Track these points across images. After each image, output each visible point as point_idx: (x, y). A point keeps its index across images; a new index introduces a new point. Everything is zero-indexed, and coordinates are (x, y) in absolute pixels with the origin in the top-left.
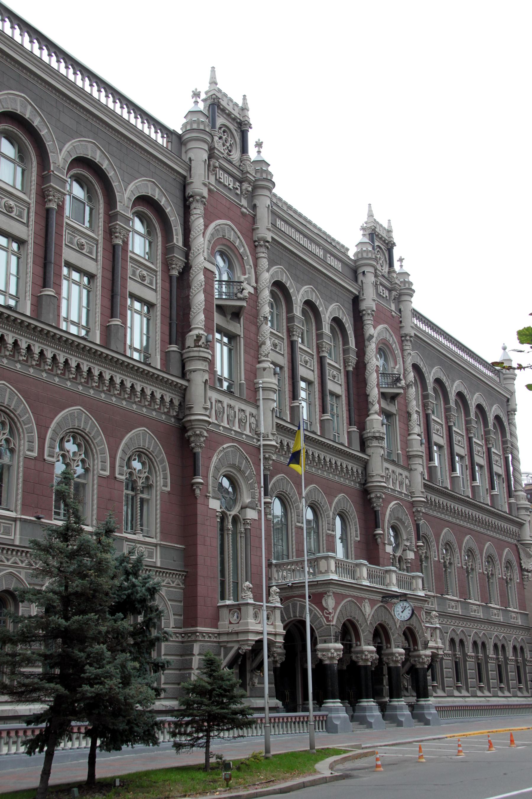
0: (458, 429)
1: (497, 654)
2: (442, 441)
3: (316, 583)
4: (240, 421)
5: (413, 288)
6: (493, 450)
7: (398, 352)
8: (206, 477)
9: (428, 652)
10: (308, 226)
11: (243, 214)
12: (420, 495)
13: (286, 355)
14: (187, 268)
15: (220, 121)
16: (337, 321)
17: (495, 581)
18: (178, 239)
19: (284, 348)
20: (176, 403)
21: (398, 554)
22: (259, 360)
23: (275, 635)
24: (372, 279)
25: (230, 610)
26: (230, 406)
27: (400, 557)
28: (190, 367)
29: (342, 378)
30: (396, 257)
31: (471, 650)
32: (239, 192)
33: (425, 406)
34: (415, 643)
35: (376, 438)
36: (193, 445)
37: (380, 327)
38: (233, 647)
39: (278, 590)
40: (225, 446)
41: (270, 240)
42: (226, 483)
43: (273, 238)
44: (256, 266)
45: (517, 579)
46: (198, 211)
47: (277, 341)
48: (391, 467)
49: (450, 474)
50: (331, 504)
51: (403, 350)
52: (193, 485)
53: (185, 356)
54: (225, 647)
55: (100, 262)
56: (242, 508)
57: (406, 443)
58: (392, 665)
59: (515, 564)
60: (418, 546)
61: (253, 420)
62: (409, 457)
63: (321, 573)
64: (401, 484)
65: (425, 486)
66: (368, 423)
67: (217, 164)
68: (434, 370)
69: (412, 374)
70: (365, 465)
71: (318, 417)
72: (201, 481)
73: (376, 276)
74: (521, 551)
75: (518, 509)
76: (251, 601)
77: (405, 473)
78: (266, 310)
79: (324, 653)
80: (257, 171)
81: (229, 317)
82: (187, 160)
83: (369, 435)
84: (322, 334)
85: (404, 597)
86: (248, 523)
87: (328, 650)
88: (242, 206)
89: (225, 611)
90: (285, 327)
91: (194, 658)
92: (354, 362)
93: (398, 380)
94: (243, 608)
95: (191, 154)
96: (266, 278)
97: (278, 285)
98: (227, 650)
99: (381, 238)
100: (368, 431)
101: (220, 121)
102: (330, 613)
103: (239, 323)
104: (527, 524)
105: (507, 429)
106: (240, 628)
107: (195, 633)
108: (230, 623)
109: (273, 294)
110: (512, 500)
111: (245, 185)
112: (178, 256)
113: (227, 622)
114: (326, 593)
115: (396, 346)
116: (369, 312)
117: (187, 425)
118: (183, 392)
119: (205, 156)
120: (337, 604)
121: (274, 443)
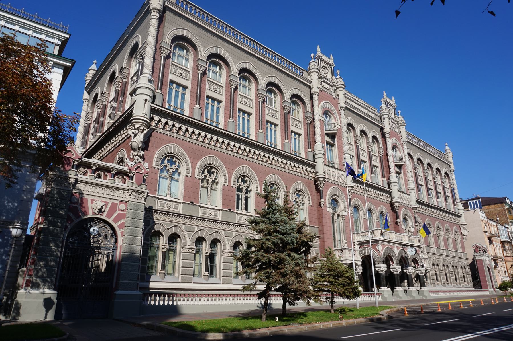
2: (423, 183)
7: (401, 148)
9: (425, 268)
12: (414, 204)
13: (354, 151)
16: (374, 138)
17: (450, 240)
18: (309, 109)
19: (354, 148)
21: (407, 230)
26: (334, 172)
28: (316, 157)
29: (378, 159)
34: (418, 264)
44: (340, 118)
47: (350, 146)
50: (377, 209)
55: (280, 120)
64: (406, 201)
65: (417, 201)
69: (407, 157)
70: (390, 193)
71: (369, 175)
73: (389, 119)
74: (461, 227)
76: (347, 248)
78: (345, 134)
81: (331, 137)
83: (391, 181)
85: (411, 246)
93: (402, 159)
94: (343, 250)
95: (312, 77)
96: (345, 122)
102: (380, 252)
105: (451, 178)
109: (348, 128)
110: (455, 207)
115: (400, 146)
119: (317, 77)
120: (383, 248)
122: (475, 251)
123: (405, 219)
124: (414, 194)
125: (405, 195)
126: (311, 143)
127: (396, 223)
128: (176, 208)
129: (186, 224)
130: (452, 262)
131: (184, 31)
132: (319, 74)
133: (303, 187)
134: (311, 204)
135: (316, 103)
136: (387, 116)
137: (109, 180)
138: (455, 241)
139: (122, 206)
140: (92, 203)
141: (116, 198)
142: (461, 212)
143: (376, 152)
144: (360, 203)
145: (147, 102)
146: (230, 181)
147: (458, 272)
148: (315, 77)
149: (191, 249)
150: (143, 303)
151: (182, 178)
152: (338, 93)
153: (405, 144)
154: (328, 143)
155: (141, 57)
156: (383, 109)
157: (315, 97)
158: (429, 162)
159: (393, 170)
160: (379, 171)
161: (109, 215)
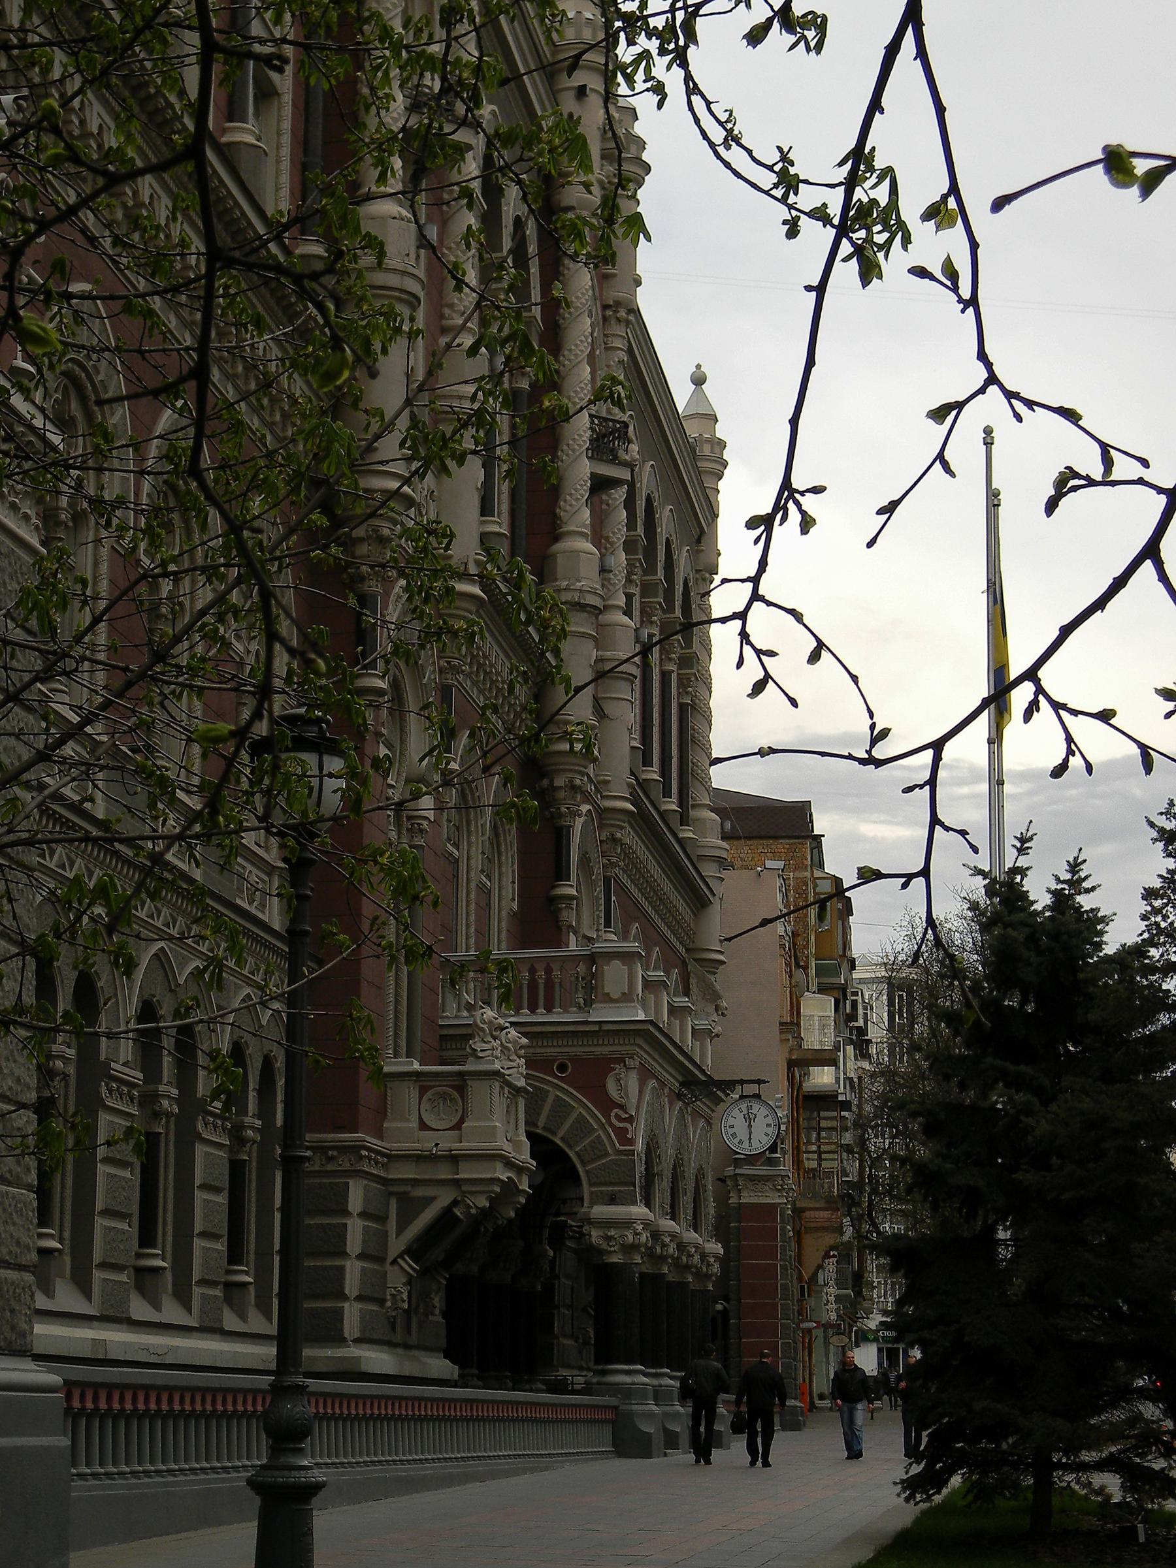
3: (596, 1028)
22: (444, 322)
23: (520, 1170)
25: (423, 1091)
38: (433, 1199)
54: (403, 1198)
63: (608, 999)
66: (560, 559)
79: (612, 1233)
86: (421, 831)
87: (627, 1224)
89: (409, 1095)
91: (349, 1222)
94: (476, 1088)
98: (409, 1208)
100: (564, 584)
106: (465, 1144)
107: (354, 1150)
108: (423, 1126)
113: (415, 1124)
114: (622, 1060)
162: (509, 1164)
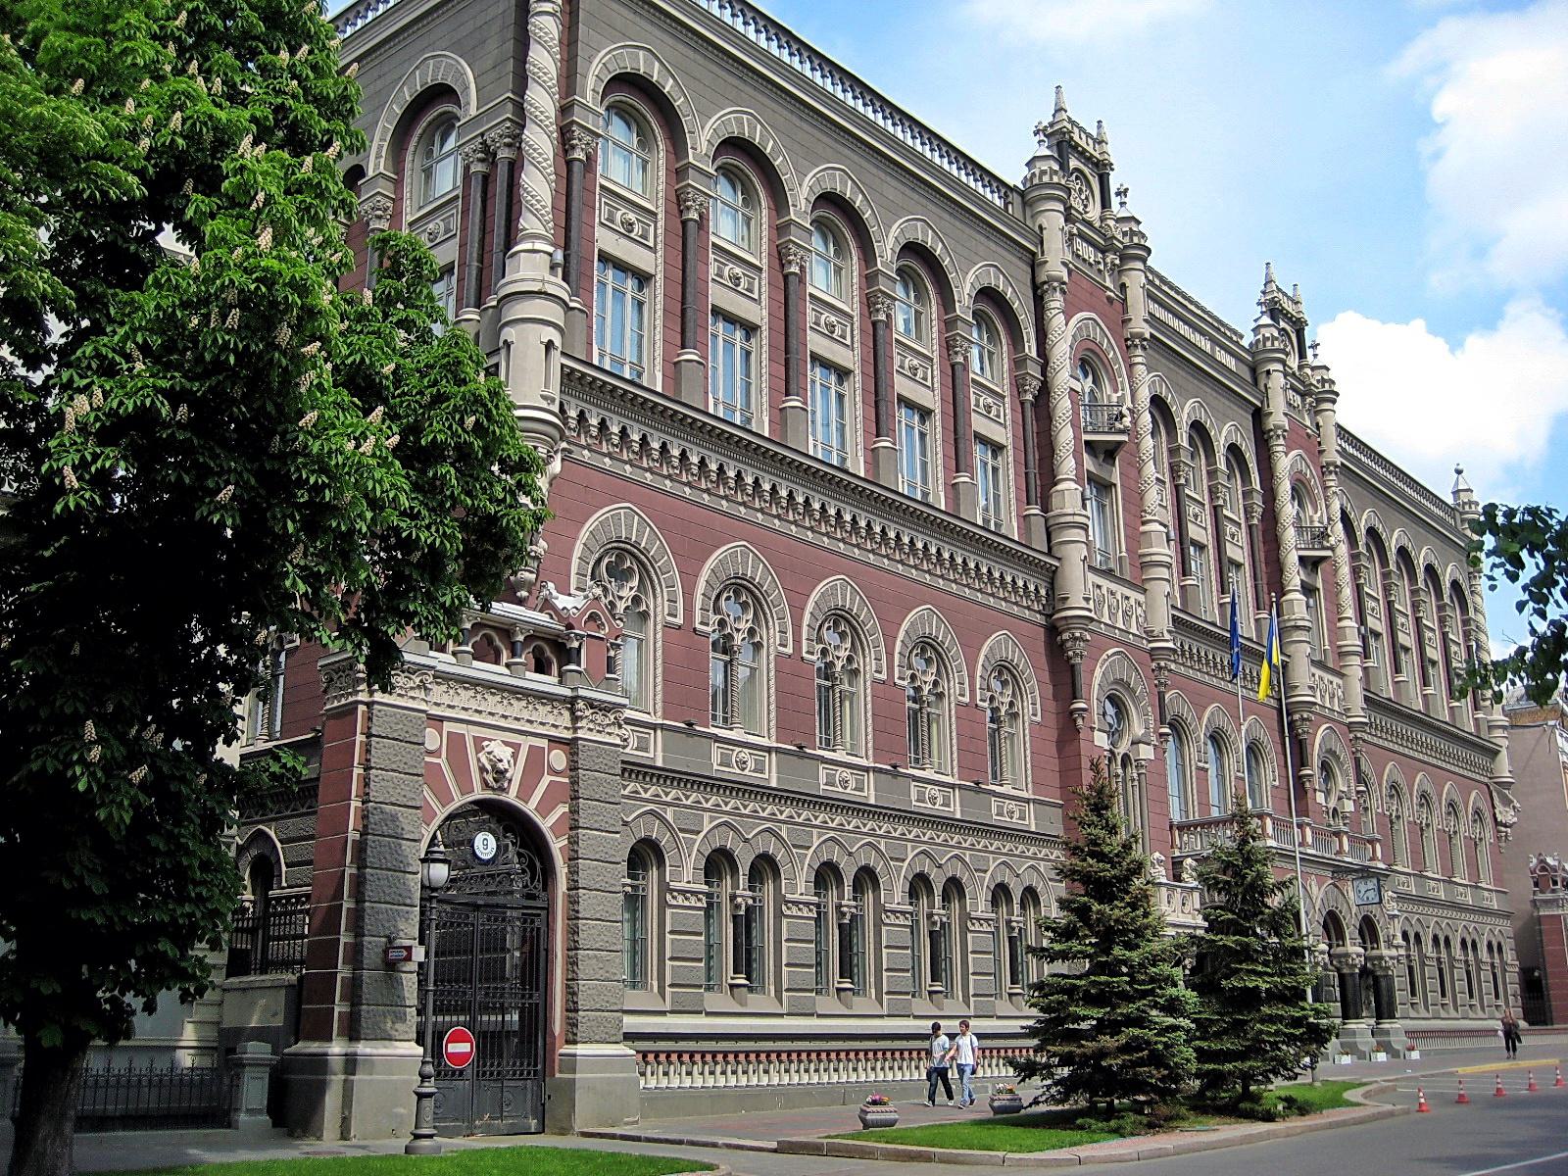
0: (1403, 605)
1: (1492, 957)
2: (1380, 627)
4: (1125, 613)
5: (1335, 389)
6: (1451, 636)
7: (1318, 491)
8: (1088, 700)
10: (1192, 307)
11: (1109, 298)
12: (1359, 713)
14: (1045, 391)
15: (1073, 163)
16: (1233, 450)
18: (1031, 349)
20: (1043, 592)
21: (1332, 805)
23: (1195, 928)
24: (1283, 381)
27: (1335, 809)
29: (1243, 537)
30: (1308, 343)
31: (1430, 949)
32: (1102, 267)
33: (1356, 572)
34: (1375, 939)
35: (1298, 628)
36: (1071, 653)
37: (1294, 453)
39: (1194, 864)
40: (1110, 652)
41: (1147, 336)
42: (1111, 710)
43: (1152, 335)
44: (1130, 376)
45: (1489, 835)
46: (1057, 304)
48: (1318, 672)
49: (1393, 678)
51: (1326, 488)
52: (1072, 712)
53: (1051, 522)
56: (1133, 743)
57: (1336, 633)
58: (1346, 971)
59: (1487, 815)
60: (1358, 792)
61: (1139, 610)
62: (1342, 655)
64: (1332, 698)
65: (1367, 699)
67: (1075, 231)
68: (1365, 516)
69: (1340, 526)
71: (1215, 599)
72: (1083, 706)
75: (1490, 728)
77: (1336, 680)
80: (1125, 234)
81: (1102, 457)
82: (1037, 229)
84: (1216, 471)
88: (1107, 288)
90: (1166, 465)
92: (1260, 510)
95: (1042, 220)
96: (1144, 395)
97: (1157, 402)
99: (1285, 315)
101: (1073, 163)
103: (1114, 465)
104: (1504, 752)
110: (1480, 715)
111: (1110, 257)
112: (1034, 370)
115: (1315, 482)
116: (1279, 432)
117: (1059, 624)
118: (1052, 576)
121: (1170, 645)
122: (1536, 884)
123: (1325, 767)
124: (1354, 667)
125: (1327, 677)
126: (1041, 480)
127: (1300, 782)
128: (643, 747)
129: (717, 812)
130: (1460, 927)
131: (637, 55)
132: (1068, 208)
133: (1014, 652)
134: (1038, 719)
135: (1056, 321)
136: (1280, 367)
137: (508, 666)
138: (1475, 844)
139: (558, 759)
140: (479, 749)
141: (541, 730)
142: (1500, 739)
143: (1233, 512)
144: (1187, 713)
145: (553, 352)
146: (797, 642)
147: (1478, 962)
148: (1053, 220)
149: (694, 893)
150: (642, 1083)
151: (654, 633)
152: (1125, 279)
153: (1333, 477)
154: (1092, 479)
155: (480, 155)
156: (1266, 339)
157: (1055, 303)
158: (1405, 542)
159: (1294, 576)
160: (1243, 584)
161: (525, 793)
162: (1175, 926)
